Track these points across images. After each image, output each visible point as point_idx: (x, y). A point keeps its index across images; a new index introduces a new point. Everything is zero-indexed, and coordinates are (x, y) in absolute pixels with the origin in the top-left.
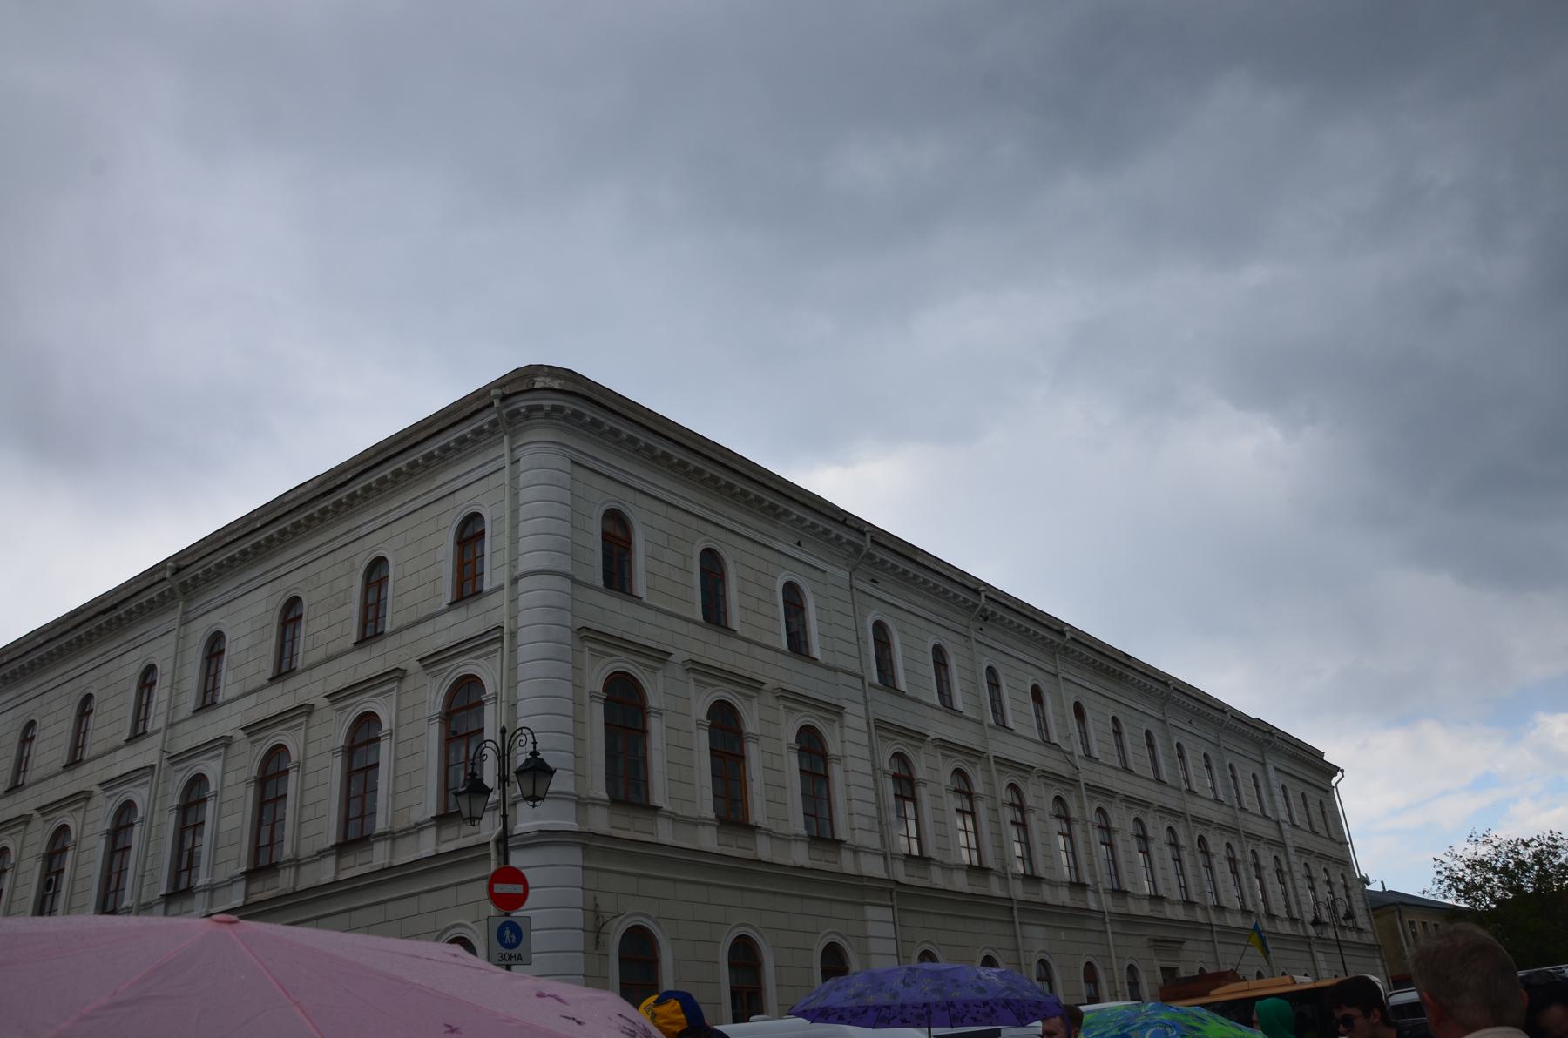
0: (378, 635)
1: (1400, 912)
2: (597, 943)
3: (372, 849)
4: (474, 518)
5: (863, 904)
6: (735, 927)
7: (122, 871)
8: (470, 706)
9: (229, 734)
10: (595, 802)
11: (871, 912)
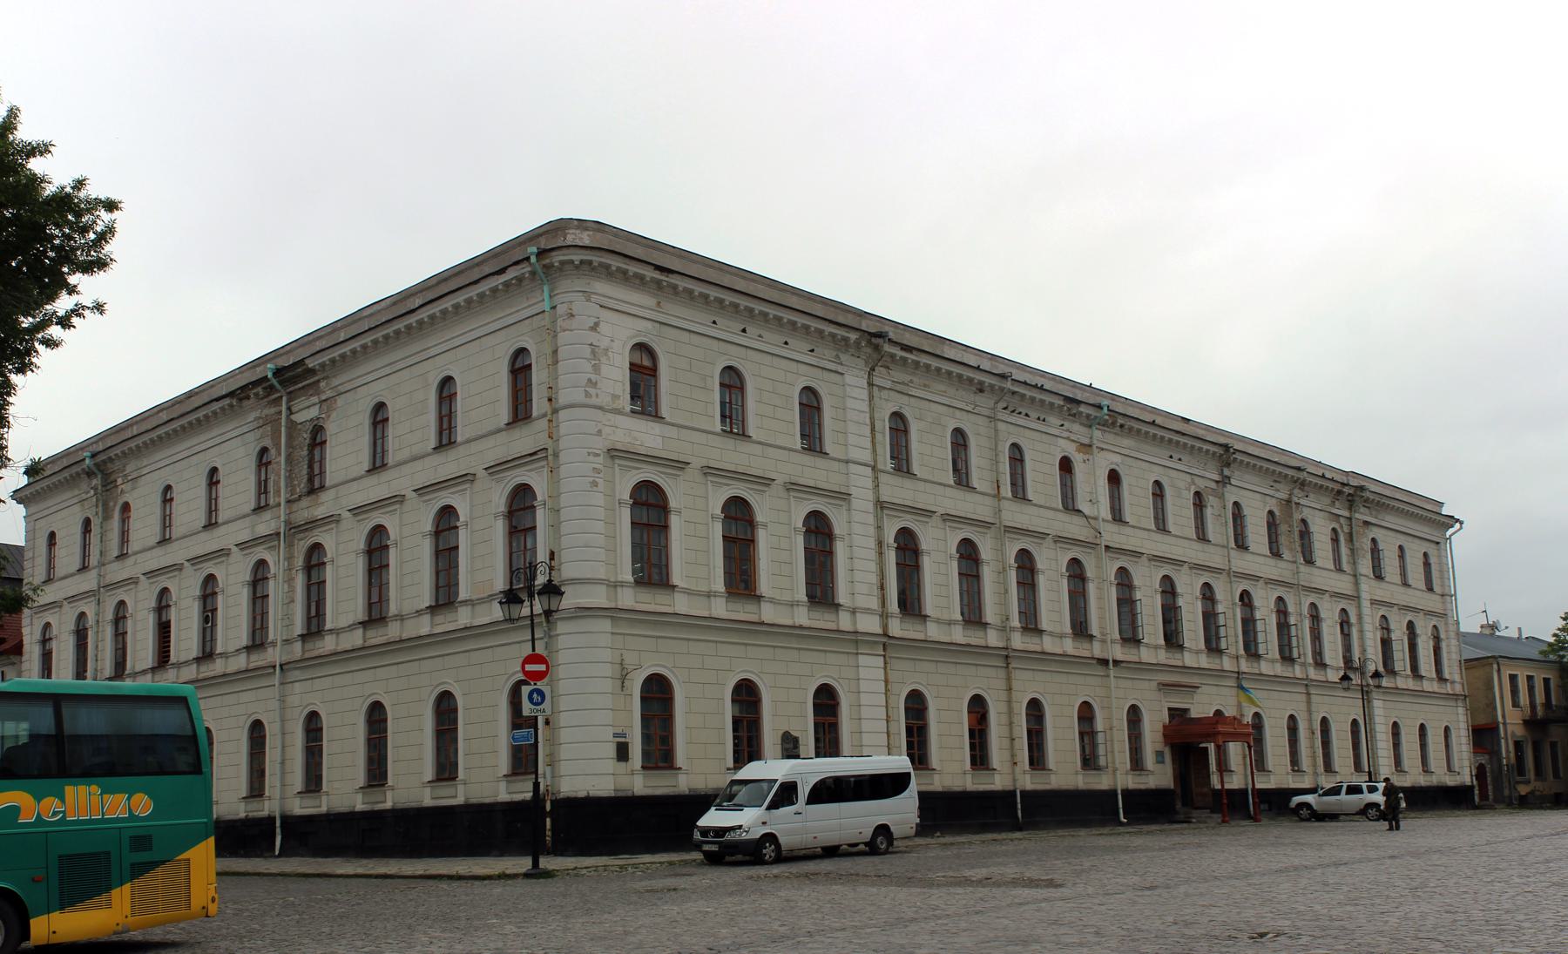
0: (451, 443)
1: (1498, 664)
2: (623, 687)
3: (457, 611)
4: (521, 352)
5: (857, 654)
6: (738, 673)
7: (264, 614)
8: (528, 508)
9: (338, 513)
10: (622, 584)
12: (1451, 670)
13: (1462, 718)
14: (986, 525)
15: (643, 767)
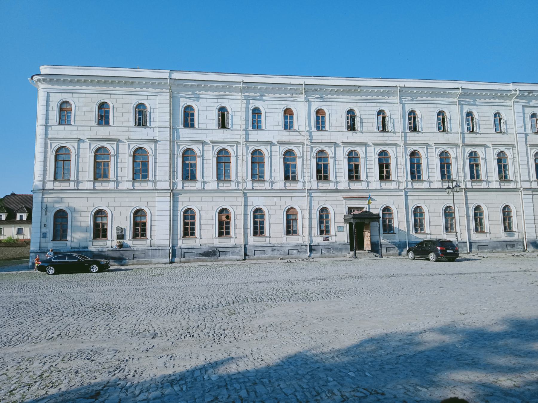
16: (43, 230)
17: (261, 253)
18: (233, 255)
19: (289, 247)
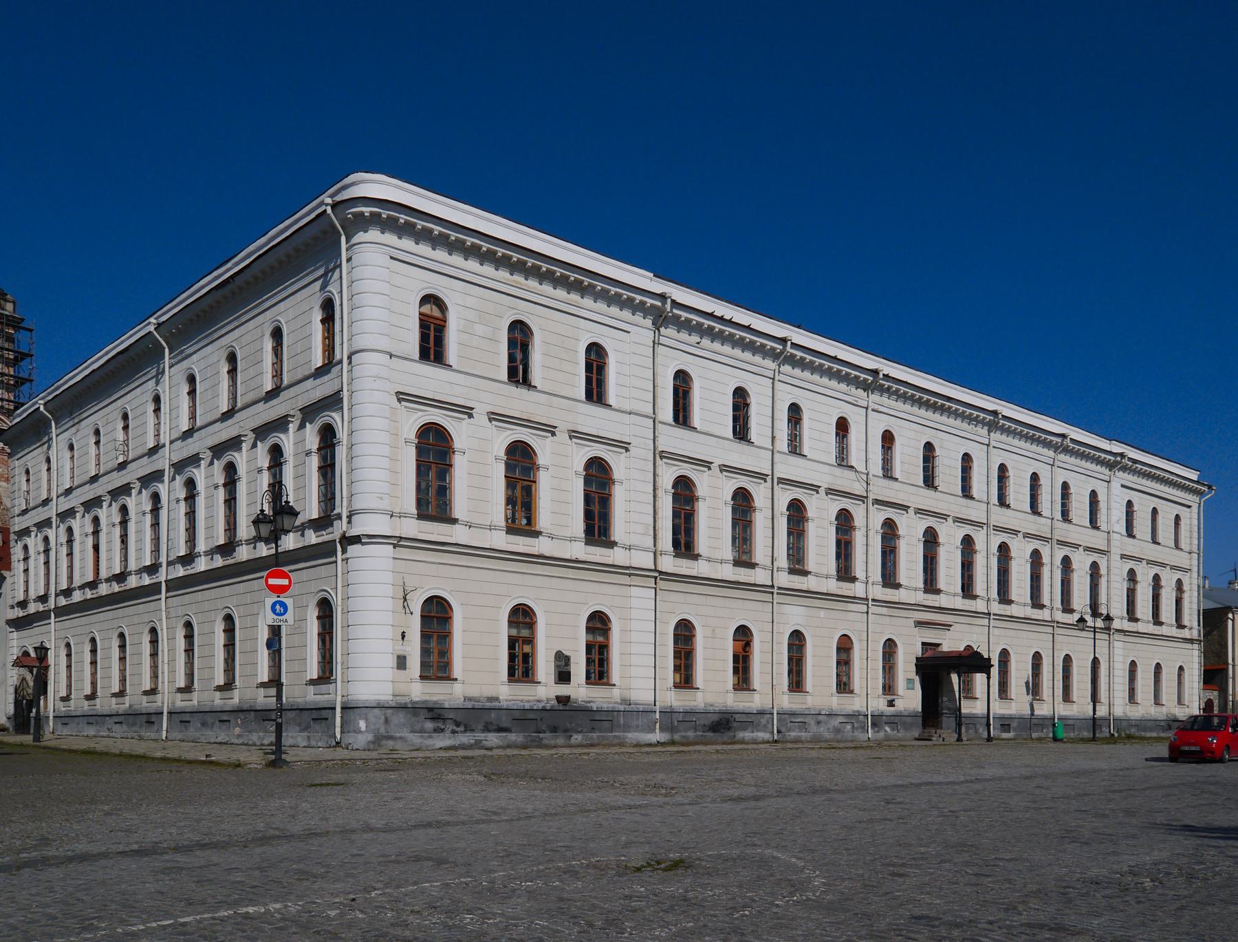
11: (635, 591)
12: (1191, 617)
13: (1196, 660)
14: (762, 477)
15: (422, 677)
16: (401, 649)
17: (800, 729)
18: (758, 731)
19: (840, 717)
